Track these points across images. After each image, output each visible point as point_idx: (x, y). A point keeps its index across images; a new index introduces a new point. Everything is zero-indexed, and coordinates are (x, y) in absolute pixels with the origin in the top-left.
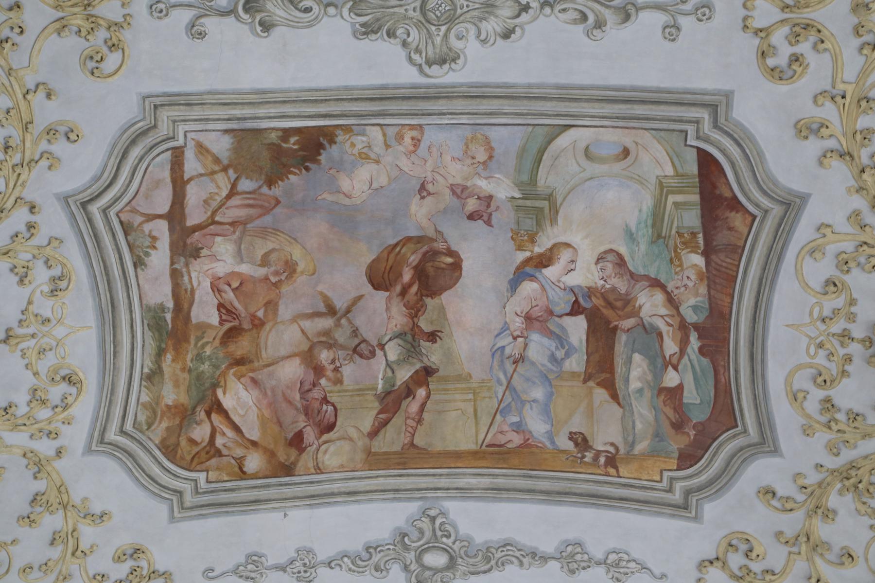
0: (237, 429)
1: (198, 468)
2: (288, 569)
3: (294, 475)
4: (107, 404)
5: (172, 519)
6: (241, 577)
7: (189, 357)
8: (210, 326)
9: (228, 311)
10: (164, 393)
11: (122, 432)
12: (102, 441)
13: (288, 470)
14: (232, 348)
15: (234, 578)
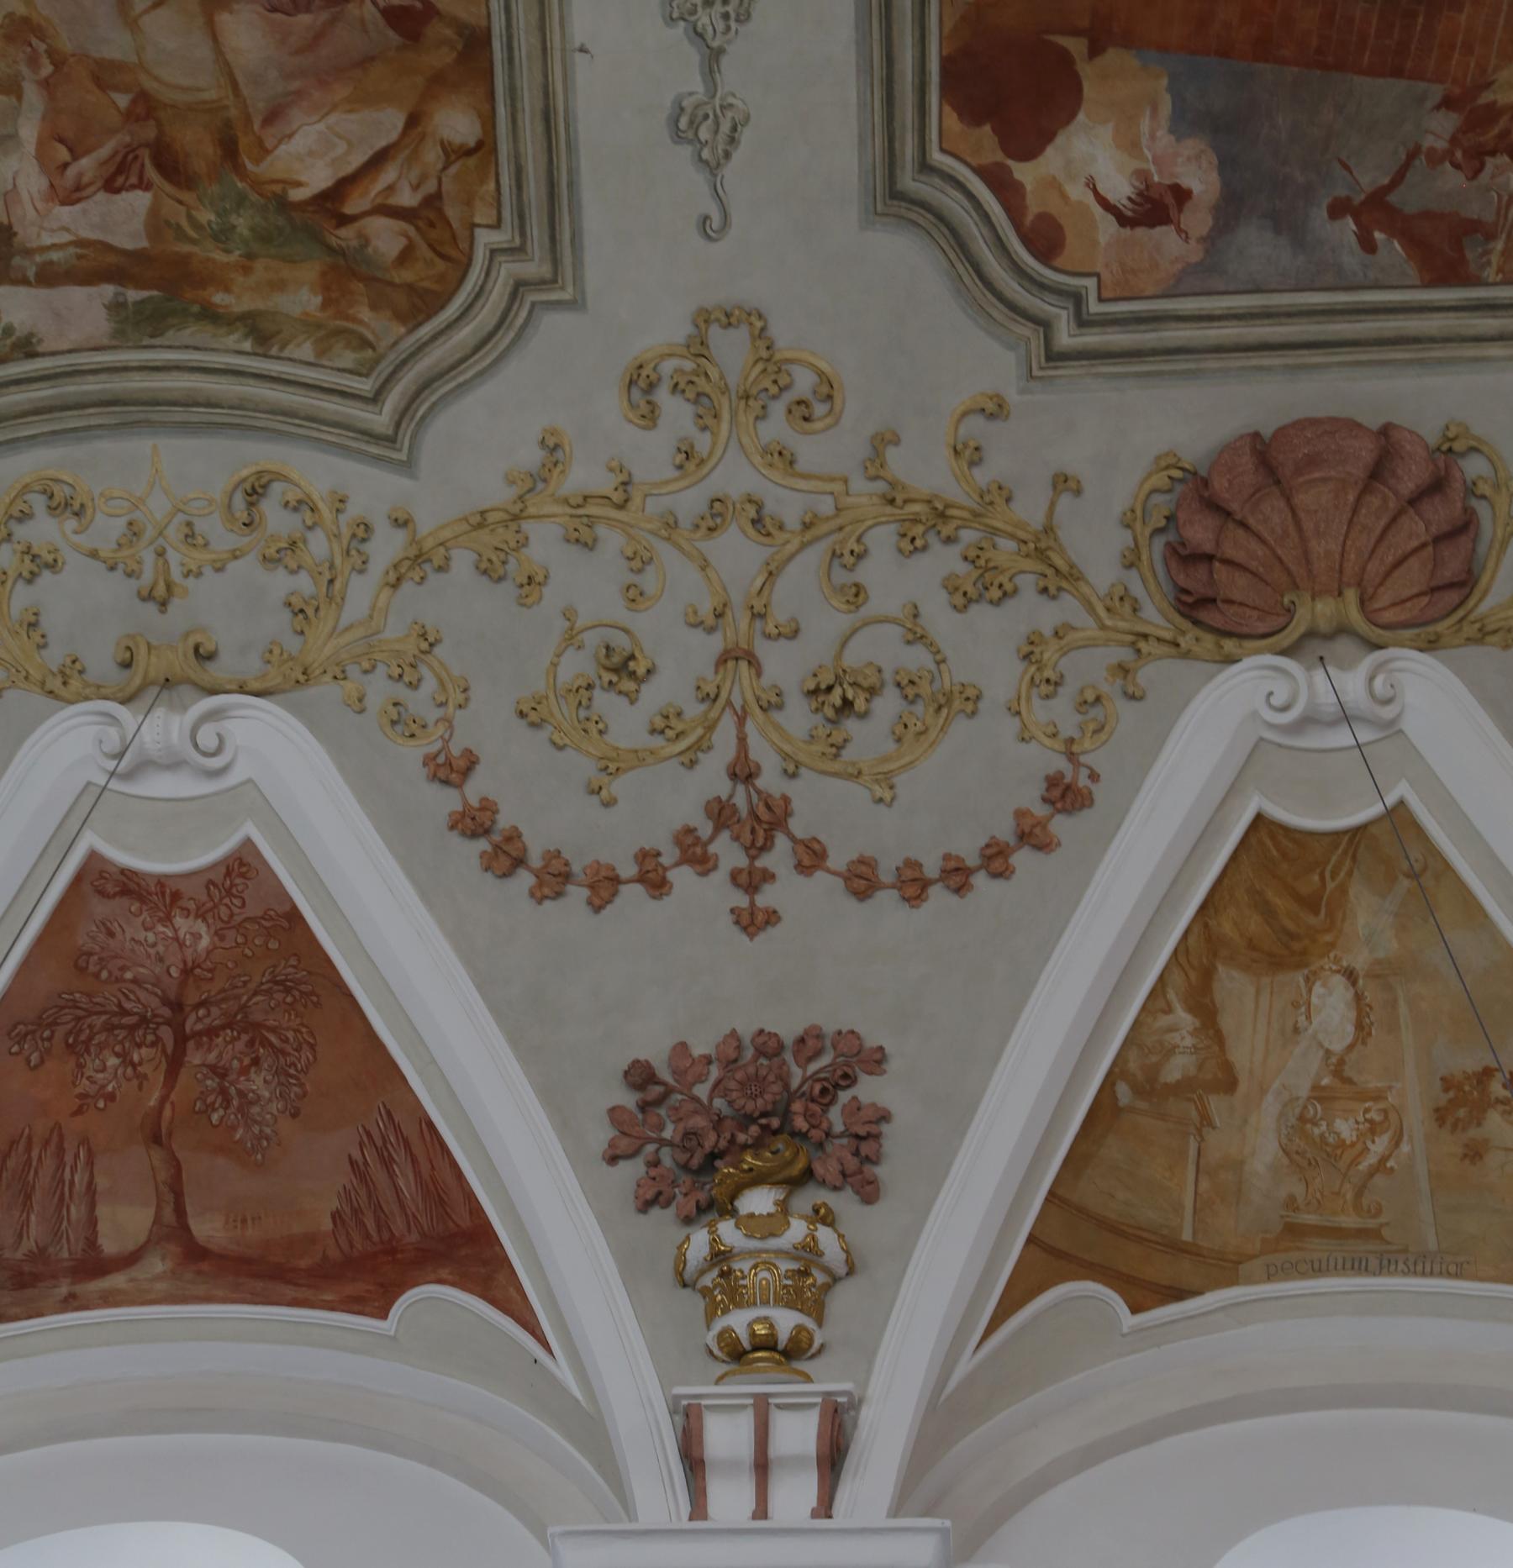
1: (464, 245)
2: (715, 44)
3: (489, 29)
4: (314, 425)
5: (576, 304)
6: (727, 155)
7: (219, 256)
8: (154, 212)
9: (122, 168)
10: (296, 311)
11: (376, 398)
12: (391, 440)
14: (199, 166)
15: (729, 172)
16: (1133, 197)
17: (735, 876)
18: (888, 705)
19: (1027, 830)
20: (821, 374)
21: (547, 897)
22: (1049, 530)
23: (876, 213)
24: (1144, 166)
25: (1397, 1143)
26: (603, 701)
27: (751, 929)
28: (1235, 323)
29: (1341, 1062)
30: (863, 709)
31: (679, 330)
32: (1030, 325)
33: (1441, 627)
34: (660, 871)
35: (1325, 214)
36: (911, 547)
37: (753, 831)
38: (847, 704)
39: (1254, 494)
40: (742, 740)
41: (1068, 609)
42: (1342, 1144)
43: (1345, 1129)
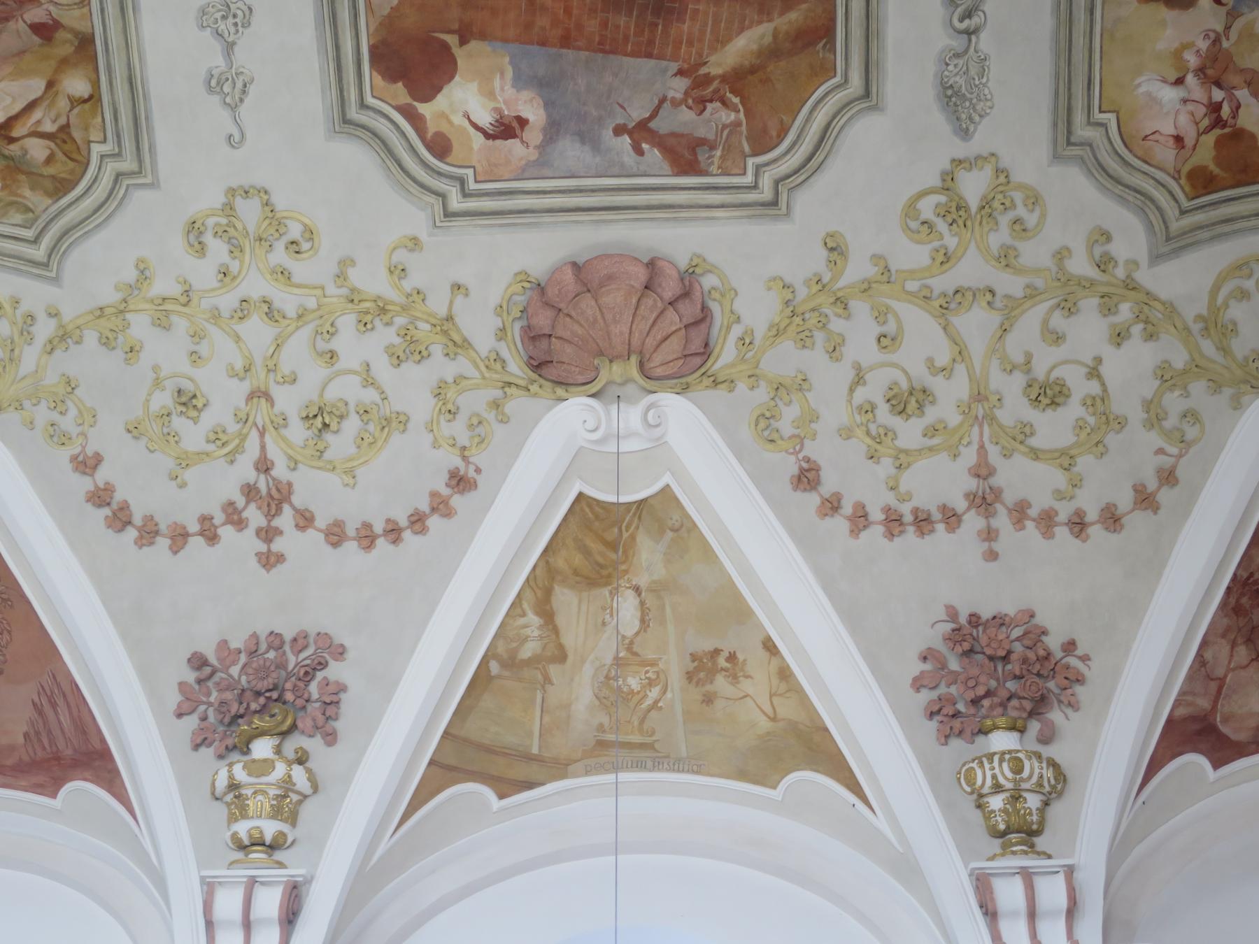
0: (31, 106)
1: (84, 153)
2: (230, 40)
3: (93, 34)
5: (154, 185)
6: (241, 100)
11: (36, 241)
12: (46, 265)
13: (85, 43)
15: (243, 110)
16: (493, 122)
17: (258, 532)
18: (352, 425)
19: (435, 506)
20: (305, 225)
21: (144, 545)
22: (449, 318)
23: (335, 132)
24: (498, 106)
25: (664, 692)
26: (178, 423)
27: (268, 567)
28: (560, 195)
29: (632, 643)
30: (336, 429)
31: (219, 199)
32: (433, 196)
33: (689, 379)
34: (213, 529)
35: (611, 133)
36: (364, 325)
37: (269, 505)
38: (326, 426)
39: (574, 298)
40: (263, 447)
41: (462, 365)
42: (632, 692)
43: (634, 683)
